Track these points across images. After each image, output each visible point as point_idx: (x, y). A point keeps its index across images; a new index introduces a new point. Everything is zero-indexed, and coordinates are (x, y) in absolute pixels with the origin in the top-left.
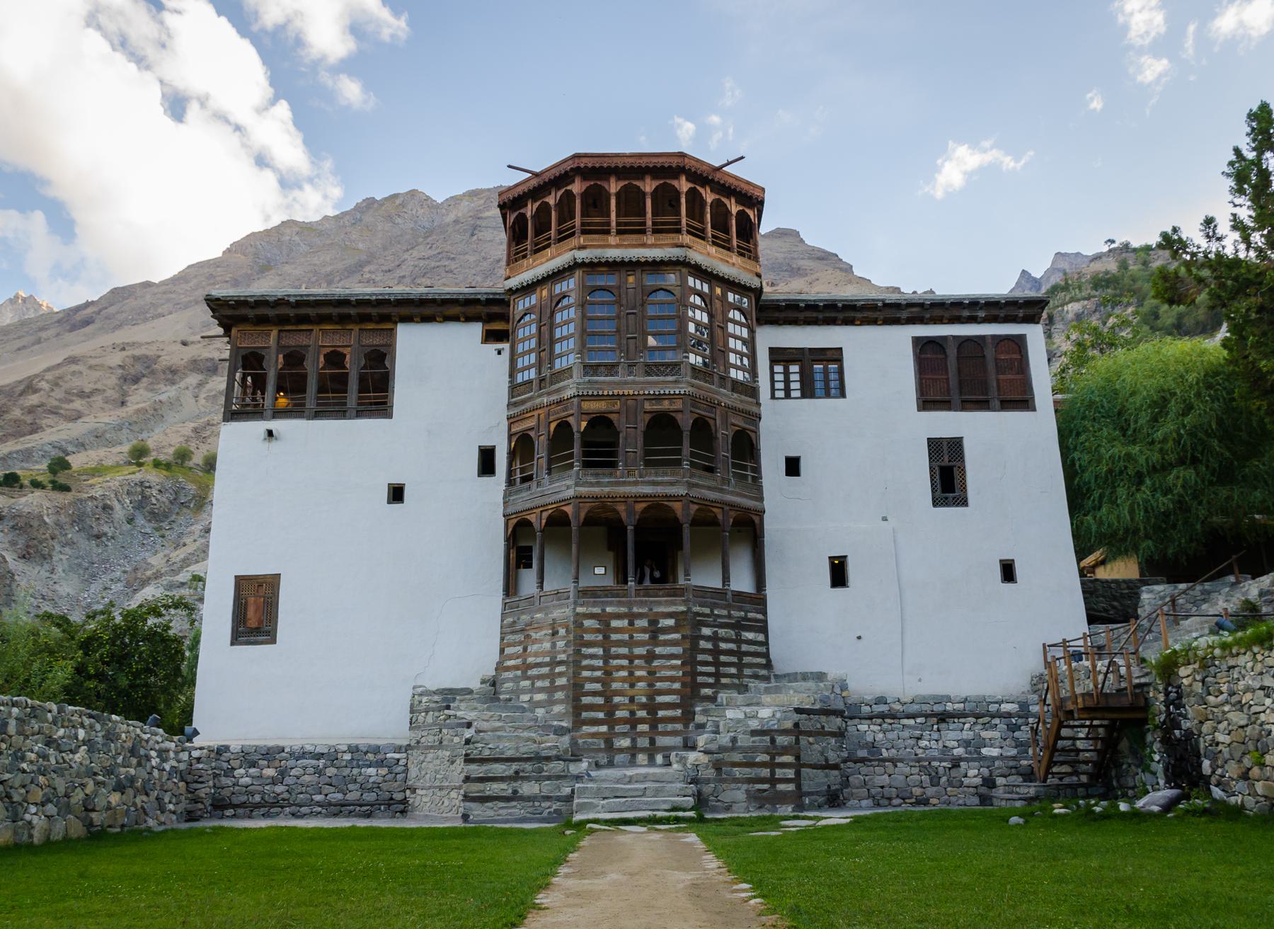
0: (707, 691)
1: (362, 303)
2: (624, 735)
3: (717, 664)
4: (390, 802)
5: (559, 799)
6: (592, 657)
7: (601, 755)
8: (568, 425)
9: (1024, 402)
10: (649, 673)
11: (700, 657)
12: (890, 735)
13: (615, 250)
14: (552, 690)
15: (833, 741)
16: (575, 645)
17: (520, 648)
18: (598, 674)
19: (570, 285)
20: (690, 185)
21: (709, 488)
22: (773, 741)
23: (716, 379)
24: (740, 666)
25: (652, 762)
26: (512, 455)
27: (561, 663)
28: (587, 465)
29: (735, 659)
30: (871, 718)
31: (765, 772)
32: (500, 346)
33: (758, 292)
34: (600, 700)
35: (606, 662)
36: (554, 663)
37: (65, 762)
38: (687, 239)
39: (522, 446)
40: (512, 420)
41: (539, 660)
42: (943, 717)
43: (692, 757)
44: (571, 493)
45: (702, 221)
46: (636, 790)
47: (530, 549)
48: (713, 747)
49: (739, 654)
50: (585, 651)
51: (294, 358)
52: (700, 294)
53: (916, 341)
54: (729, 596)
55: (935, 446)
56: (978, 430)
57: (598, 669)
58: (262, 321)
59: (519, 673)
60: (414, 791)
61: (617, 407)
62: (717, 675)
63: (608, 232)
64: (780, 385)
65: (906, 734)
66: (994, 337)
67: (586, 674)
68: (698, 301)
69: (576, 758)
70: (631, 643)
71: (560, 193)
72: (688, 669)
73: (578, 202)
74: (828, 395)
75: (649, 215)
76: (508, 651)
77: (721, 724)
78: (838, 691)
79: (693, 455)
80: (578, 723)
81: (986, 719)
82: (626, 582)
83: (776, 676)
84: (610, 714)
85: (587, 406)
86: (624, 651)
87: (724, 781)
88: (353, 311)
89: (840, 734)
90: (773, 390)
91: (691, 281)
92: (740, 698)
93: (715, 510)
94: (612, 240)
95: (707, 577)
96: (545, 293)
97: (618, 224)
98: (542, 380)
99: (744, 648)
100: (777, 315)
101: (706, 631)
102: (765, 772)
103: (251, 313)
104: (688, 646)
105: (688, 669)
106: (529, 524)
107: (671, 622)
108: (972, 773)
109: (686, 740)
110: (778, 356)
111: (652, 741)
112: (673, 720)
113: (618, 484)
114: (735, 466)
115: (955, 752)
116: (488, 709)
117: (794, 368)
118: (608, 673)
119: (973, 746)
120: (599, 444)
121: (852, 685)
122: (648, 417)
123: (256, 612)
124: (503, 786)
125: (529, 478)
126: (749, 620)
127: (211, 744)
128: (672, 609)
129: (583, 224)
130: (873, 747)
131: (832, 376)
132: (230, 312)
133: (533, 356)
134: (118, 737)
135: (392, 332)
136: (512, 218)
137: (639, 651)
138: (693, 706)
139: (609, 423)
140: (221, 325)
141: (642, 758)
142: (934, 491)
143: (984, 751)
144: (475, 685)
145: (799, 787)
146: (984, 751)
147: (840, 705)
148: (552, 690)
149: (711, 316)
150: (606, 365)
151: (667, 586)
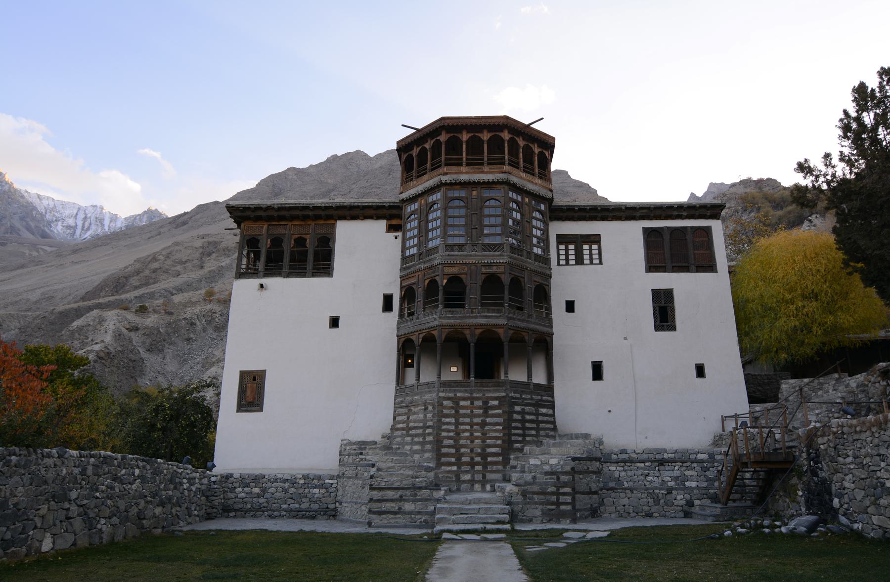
0: (517, 445)
1: (316, 208)
2: (467, 472)
3: (524, 428)
5: (427, 513)
6: (449, 424)
7: (453, 484)
8: (436, 281)
9: (709, 266)
10: (483, 434)
11: (514, 425)
12: (629, 473)
13: (465, 175)
14: (423, 444)
16: (438, 416)
17: (405, 417)
18: (452, 434)
19: (438, 196)
20: (510, 136)
21: (520, 320)
22: (558, 478)
23: (525, 253)
24: (538, 429)
25: (483, 490)
26: (402, 299)
27: (429, 427)
28: (446, 306)
29: (534, 425)
30: (617, 462)
31: (554, 498)
32: (396, 234)
33: (551, 200)
34: (453, 451)
35: (456, 427)
36: (425, 427)
37: (125, 490)
38: (508, 168)
39: (408, 294)
40: (403, 278)
41: (416, 425)
42: (662, 462)
43: (509, 487)
44: (436, 323)
45: (518, 158)
46: (474, 509)
48: (522, 482)
49: (537, 422)
51: (277, 242)
52: (516, 202)
54: (532, 387)
56: (682, 284)
57: (452, 431)
58: (258, 219)
59: (404, 432)
61: (465, 271)
62: (524, 436)
63: (461, 165)
64: (563, 257)
65: (639, 472)
66: (692, 227)
67: (444, 434)
68: (515, 206)
69: (436, 486)
70: (472, 416)
71: (432, 142)
72: (506, 431)
73: (443, 146)
74: (591, 263)
75: (486, 154)
76: (398, 418)
77: (527, 466)
78: (597, 445)
79: (510, 300)
80: (439, 464)
81: (688, 464)
82: (469, 378)
83: (560, 436)
84: (459, 459)
85: (446, 270)
86: (467, 420)
87: (528, 503)
88: (311, 213)
89: (598, 472)
90: (559, 260)
91: (510, 194)
92: (537, 450)
93: (524, 334)
94: (464, 169)
95: (517, 375)
96: (423, 202)
97: (467, 159)
98: (421, 254)
99: (540, 418)
100: (561, 214)
101: (517, 408)
102: (554, 498)
103: (252, 215)
104: (506, 417)
105: (506, 431)
106: (411, 341)
107: (496, 403)
108: (679, 497)
109: (504, 476)
110: (563, 239)
111: (484, 476)
112: (496, 463)
113: (465, 317)
115: (669, 484)
116: (386, 455)
117: (571, 247)
118: (458, 434)
119: (681, 480)
120: (454, 293)
121: (605, 440)
122: (483, 277)
124: (393, 505)
126: (544, 401)
127: (222, 473)
128: (497, 395)
129: (446, 160)
130: (618, 479)
131: (594, 252)
132: (240, 214)
133: (416, 239)
134: (162, 472)
135: (334, 225)
136: (404, 157)
137: (476, 420)
138: (509, 454)
139: (460, 280)
140: (235, 222)
141: (477, 486)
143: (687, 484)
144: (378, 438)
145: (574, 507)
146: (687, 484)
147: (599, 455)
148: (423, 444)
149: (522, 215)
150: (458, 245)
151: (494, 380)
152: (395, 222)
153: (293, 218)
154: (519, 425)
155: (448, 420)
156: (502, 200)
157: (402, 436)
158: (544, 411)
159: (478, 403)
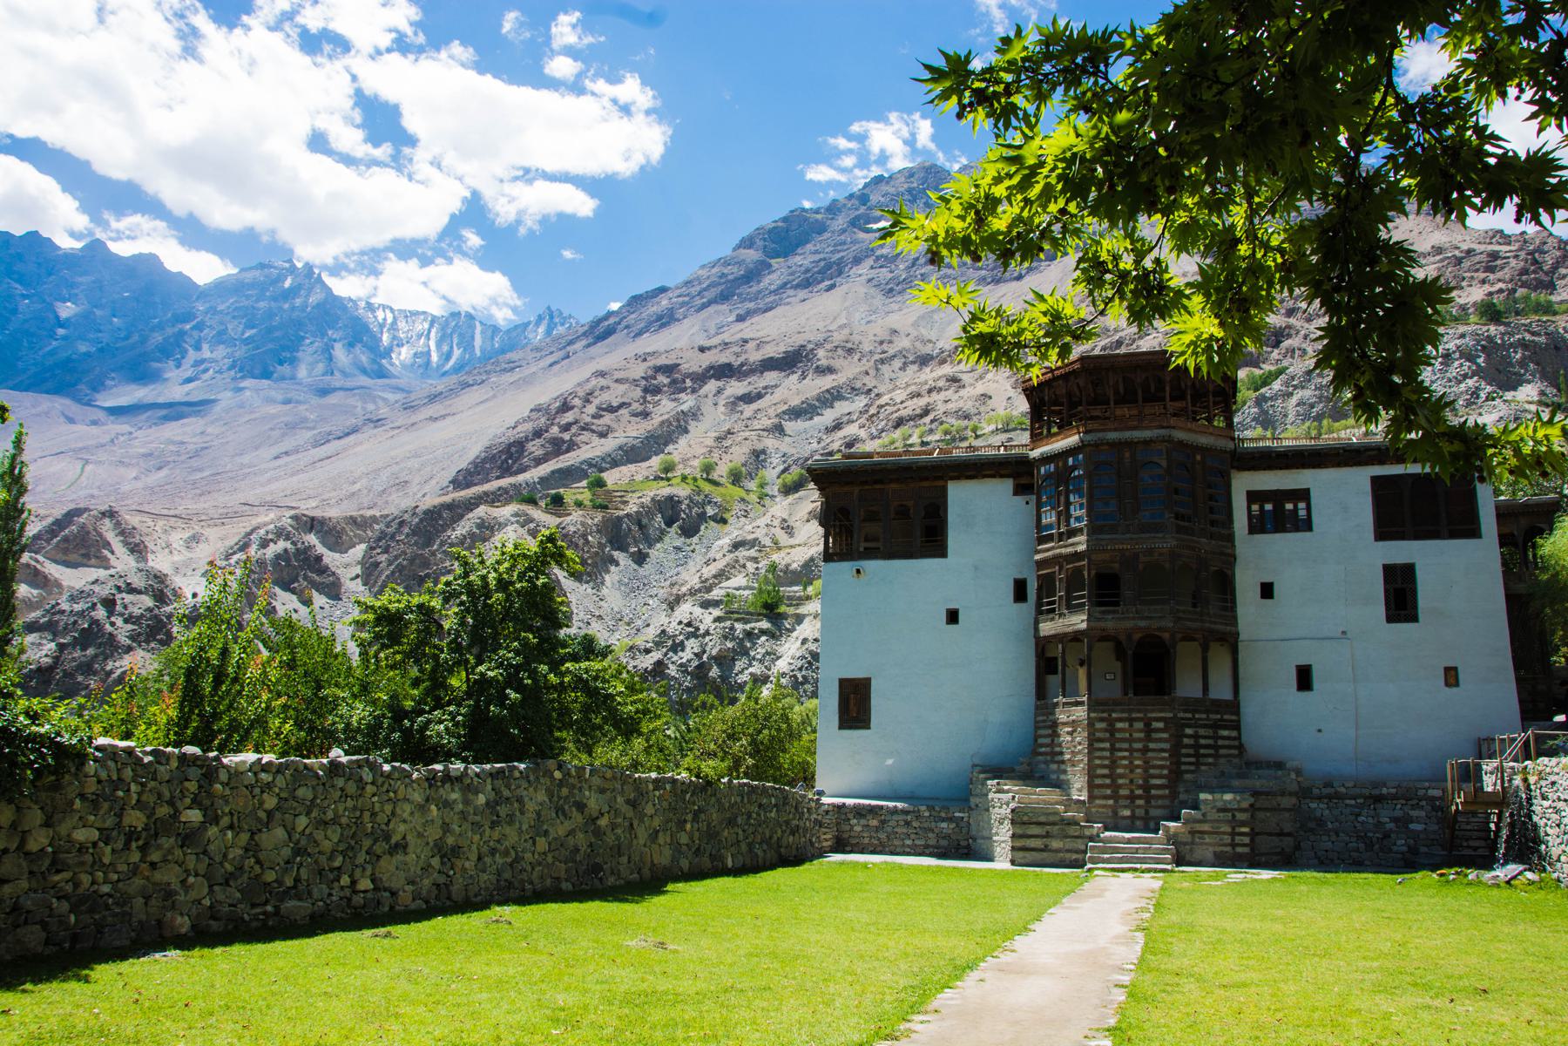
0: (1188, 776)
2: (1126, 807)
3: (1197, 755)
4: (958, 847)
6: (1103, 749)
12: (1336, 812)
15: (1287, 815)
30: (1320, 798)
31: (1227, 839)
32: (1027, 498)
34: (1108, 781)
39: (1046, 585)
42: (1379, 799)
44: (1084, 626)
49: (1216, 747)
50: (1097, 745)
53: (1375, 480)
60: (975, 840)
62: (1197, 764)
65: (1348, 811)
67: (1097, 762)
74: (1297, 530)
76: (1041, 741)
78: (1293, 776)
80: (1091, 797)
83: (1248, 764)
86: (1126, 745)
99: (1220, 742)
101: (1189, 731)
107: (1161, 725)
111: (1147, 812)
117: (1268, 507)
119: (1403, 822)
122: (1141, 567)
123: (855, 704)
125: (1053, 610)
130: (1320, 822)
143: (1412, 826)
145: (1252, 850)
146: (1412, 826)
147: (1294, 787)
152: (1023, 481)
153: (891, 481)
154: (1191, 751)
155: (1102, 745)
156: (1164, 463)
157: (1046, 762)
159: (1140, 725)
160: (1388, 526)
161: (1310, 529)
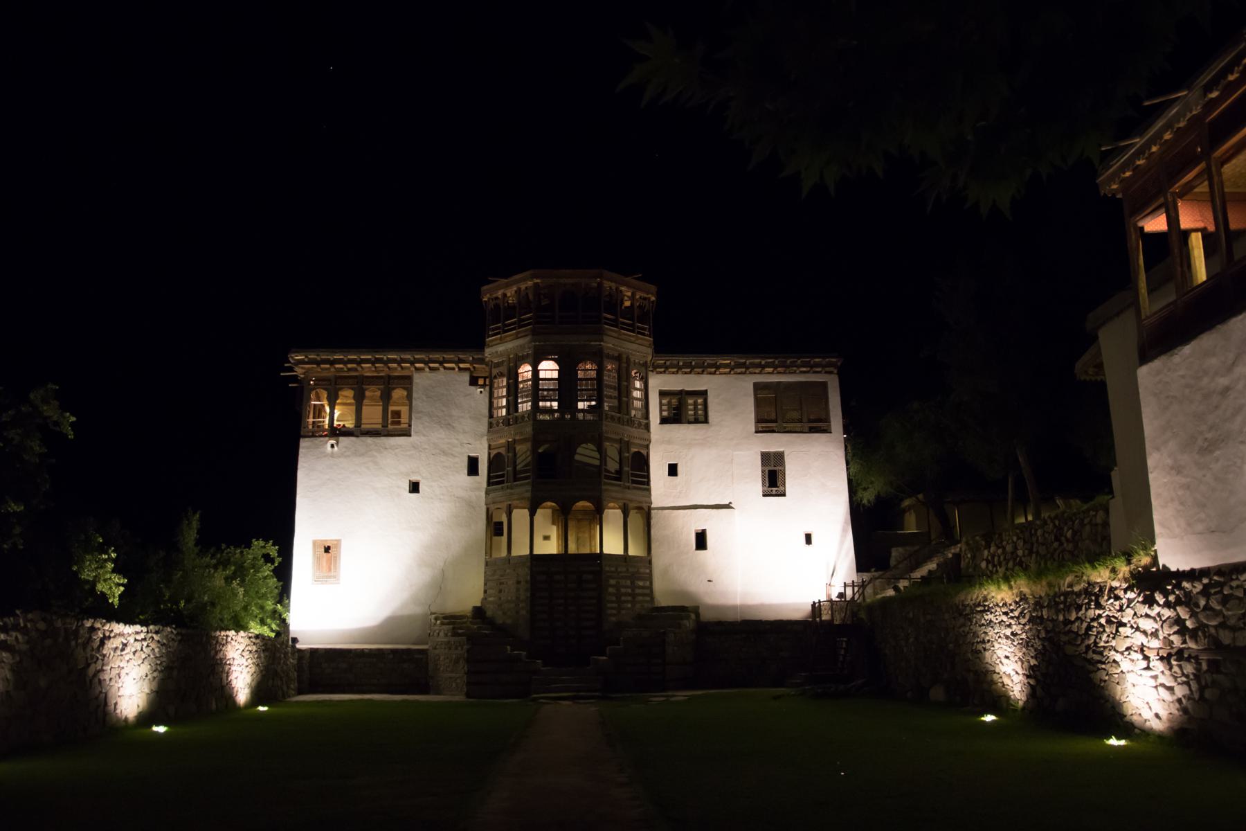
26: (490, 463)
47: (501, 523)
53: (755, 384)
55: (766, 458)
78: (693, 616)
99: (638, 591)
101: (613, 582)
110: (663, 394)
114: (633, 475)
142: (764, 485)
158: (641, 583)
160: (765, 424)
161: (706, 421)
